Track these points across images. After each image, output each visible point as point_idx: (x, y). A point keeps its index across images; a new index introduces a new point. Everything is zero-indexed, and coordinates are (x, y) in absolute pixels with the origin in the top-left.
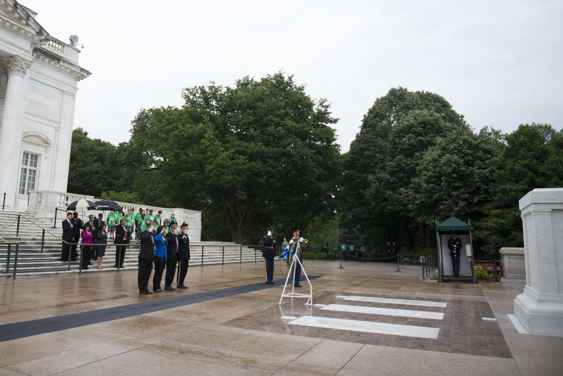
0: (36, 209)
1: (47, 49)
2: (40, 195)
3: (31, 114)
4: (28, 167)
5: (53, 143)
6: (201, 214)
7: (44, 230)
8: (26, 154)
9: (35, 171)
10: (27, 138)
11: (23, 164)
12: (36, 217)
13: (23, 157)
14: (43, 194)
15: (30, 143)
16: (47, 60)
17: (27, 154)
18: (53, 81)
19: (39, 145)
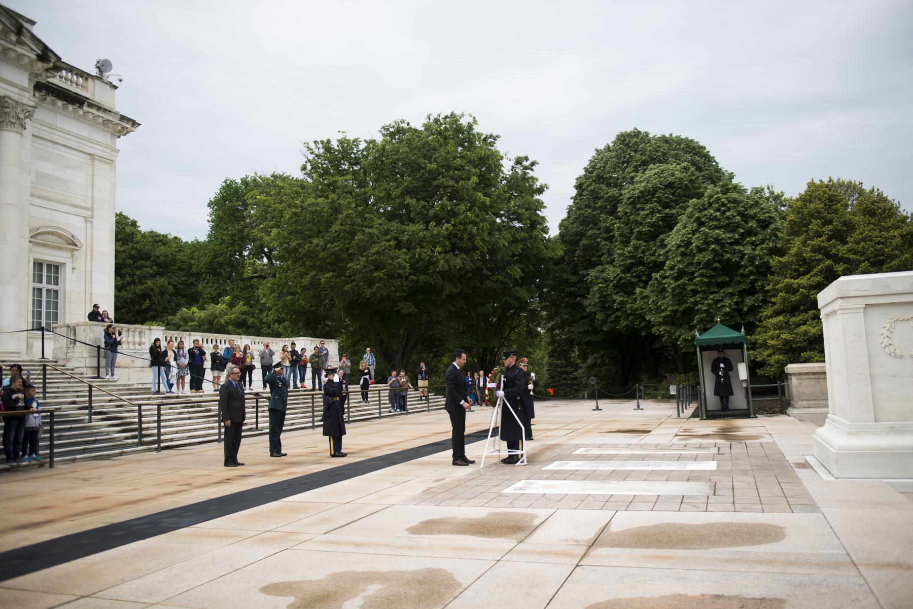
0: (68, 354)
1: (58, 84)
2: (72, 331)
3: (40, 197)
4: (44, 286)
5: (84, 243)
6: (337, 343)
7: (90, 387)
8: (38, 265)
9: (56, 292)
10: (37, 237)
12: (69, 365)
13: (34, 270)
15: (43, 245)
16: (60, 103)
18: (74, 139)
19: (60, 248)
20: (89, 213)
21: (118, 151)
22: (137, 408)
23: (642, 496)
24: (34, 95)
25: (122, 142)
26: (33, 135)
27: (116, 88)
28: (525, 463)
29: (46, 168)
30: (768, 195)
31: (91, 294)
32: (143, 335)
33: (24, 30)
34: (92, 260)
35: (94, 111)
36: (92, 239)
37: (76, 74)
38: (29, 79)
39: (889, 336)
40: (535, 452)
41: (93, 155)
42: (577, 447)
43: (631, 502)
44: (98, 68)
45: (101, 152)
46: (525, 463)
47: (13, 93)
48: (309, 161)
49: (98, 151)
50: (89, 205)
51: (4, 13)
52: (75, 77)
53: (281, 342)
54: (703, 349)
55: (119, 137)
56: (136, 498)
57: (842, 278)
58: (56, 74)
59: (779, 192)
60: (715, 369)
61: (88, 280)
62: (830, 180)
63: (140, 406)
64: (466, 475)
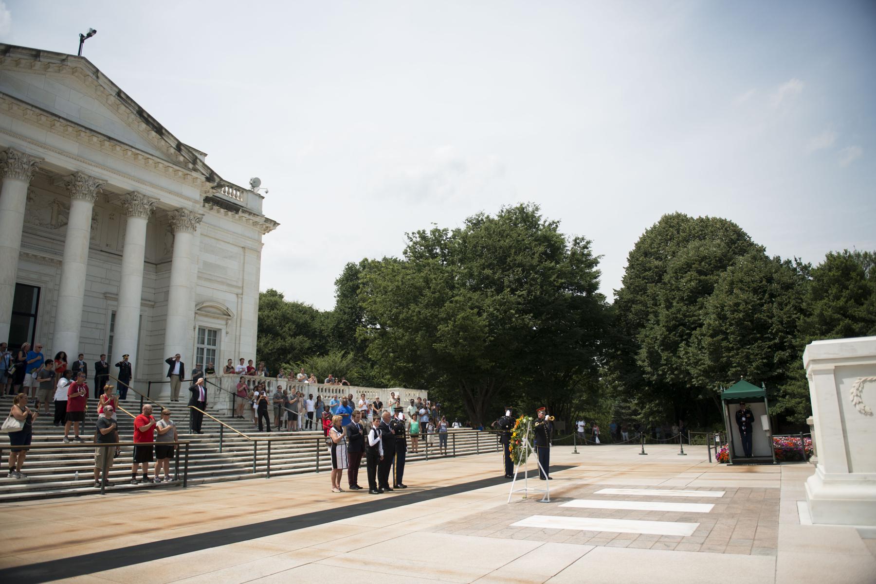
3: (207, 279)
4: (206, 346)
5: (235, 314)
8: (202, 330)
9: (214, 351)
11: (198, 343)
13: (199, 334)
14: (222, 379)
16: (222, 210)
17: (204, 330)
20: (240, 291)
21: (263, 244)
22: (253, 443)
23: (627, 534)
24: (204, 206)
25: (265, 238)
26: (201, 234)
27: (263, 198)
28: (549, 501)
29: (212, 258)
30: (795, 266)
31: (239, 352)
33: (198, 161)
34: (240, 327)
35: (246, 215)
36: (241, 311)
37: (235, 189)
38: (201, 195)
39: (859, 395)
40: (562, 490)
42: (602, 487)
43: (613, 539)
44: (251, 184)
46: (549, 501)
47: (187, 205)
48: (409, 246)
49: (249, 243)
50: (240, 285)
51: (185, 150)
52: (234, 191)
54: (728, 402)
55: (264, 234)
56: (228, 514)
57: (814, 343)
58: (219, 190)
59: (807, 264)
60: (738, 420)
61: (237, 342)
62: (846, 251)
63: (256, 441)
64: (491, 509)
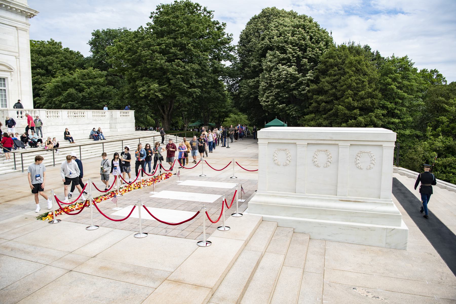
9: (5, 90)
14: (4, 111)
19: (4, 71)
20: (17, 55)
31: (21, 91)
32: (36, 113)
34: (20, 76)
36: (20, 66)
41: (17, 27)
45: (21, 26)
50: (18, 51)
53: (107, 112)
